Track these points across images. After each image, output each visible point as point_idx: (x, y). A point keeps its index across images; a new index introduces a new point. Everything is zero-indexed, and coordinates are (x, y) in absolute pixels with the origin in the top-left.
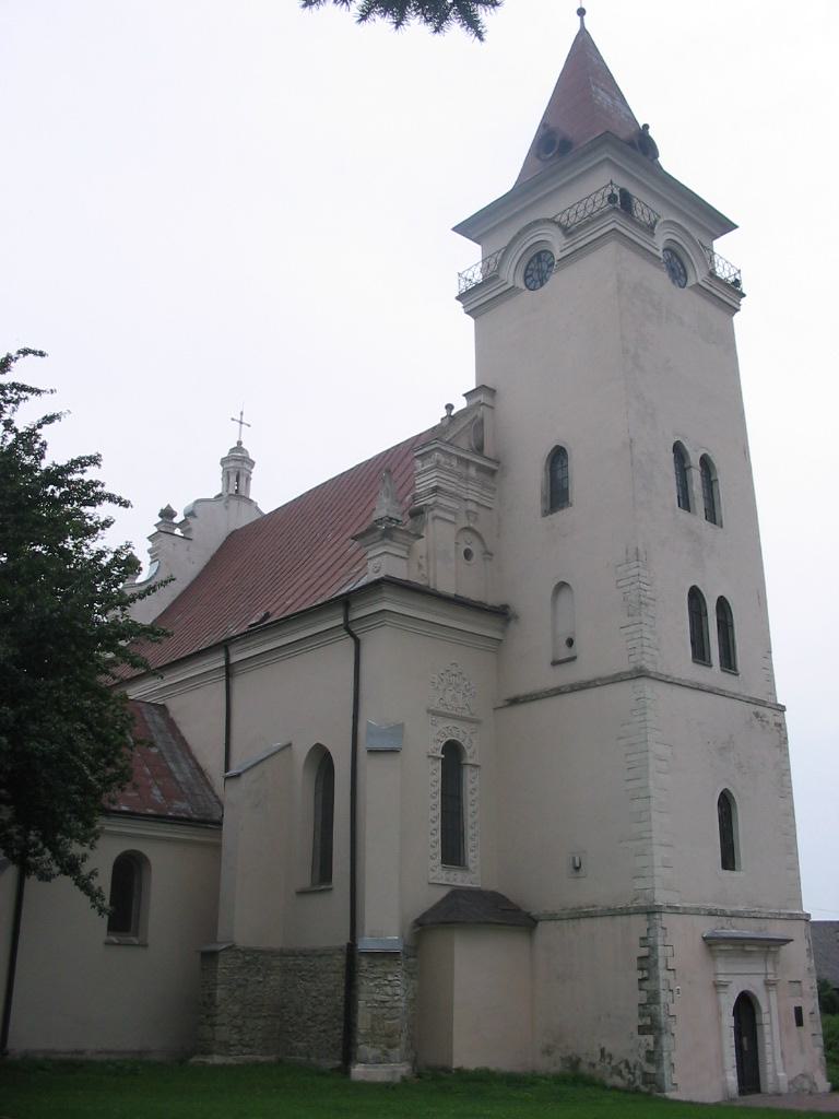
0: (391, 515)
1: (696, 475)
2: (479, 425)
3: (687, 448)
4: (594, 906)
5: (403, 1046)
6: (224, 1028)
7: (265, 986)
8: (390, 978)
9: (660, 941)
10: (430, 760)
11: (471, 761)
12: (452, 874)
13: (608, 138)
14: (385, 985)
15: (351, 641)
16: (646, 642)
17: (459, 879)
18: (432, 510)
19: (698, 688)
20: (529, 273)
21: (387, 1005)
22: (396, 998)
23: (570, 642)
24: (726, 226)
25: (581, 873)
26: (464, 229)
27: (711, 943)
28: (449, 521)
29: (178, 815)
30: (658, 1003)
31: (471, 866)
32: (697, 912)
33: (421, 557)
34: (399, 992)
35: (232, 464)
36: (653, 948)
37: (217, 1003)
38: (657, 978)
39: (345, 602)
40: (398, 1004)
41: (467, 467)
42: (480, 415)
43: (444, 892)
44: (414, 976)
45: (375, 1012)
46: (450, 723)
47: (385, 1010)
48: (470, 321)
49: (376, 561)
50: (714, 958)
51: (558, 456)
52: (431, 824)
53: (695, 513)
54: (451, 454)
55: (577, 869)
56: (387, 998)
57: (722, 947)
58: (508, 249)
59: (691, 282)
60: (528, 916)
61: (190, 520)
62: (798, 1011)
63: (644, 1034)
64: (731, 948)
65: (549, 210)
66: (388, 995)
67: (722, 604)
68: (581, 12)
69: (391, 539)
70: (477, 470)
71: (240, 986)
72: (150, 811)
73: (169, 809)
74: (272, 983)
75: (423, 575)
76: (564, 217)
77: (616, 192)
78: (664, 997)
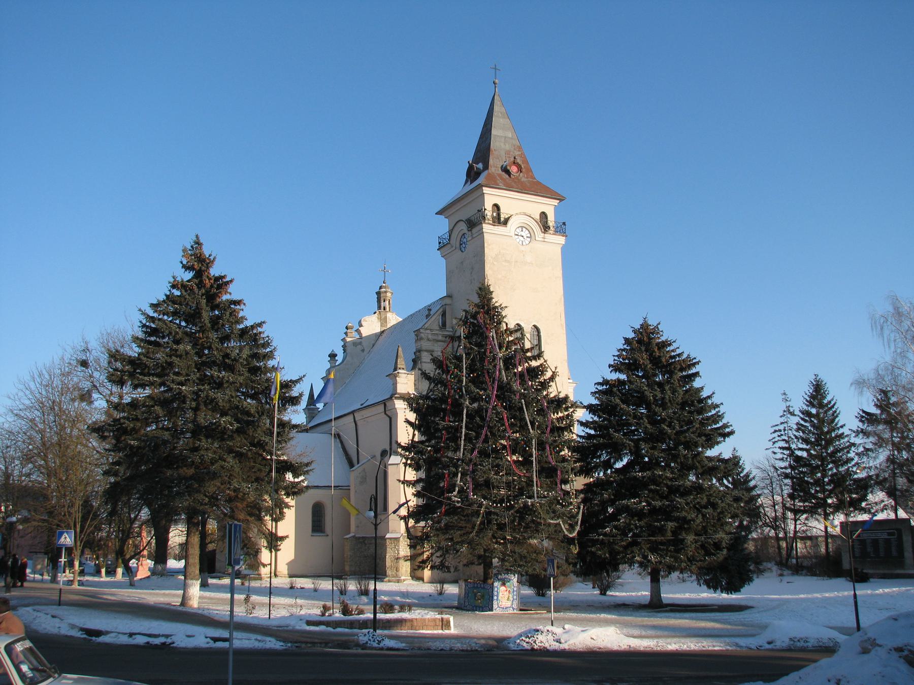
26: (439, 213)
48: (443, 261)
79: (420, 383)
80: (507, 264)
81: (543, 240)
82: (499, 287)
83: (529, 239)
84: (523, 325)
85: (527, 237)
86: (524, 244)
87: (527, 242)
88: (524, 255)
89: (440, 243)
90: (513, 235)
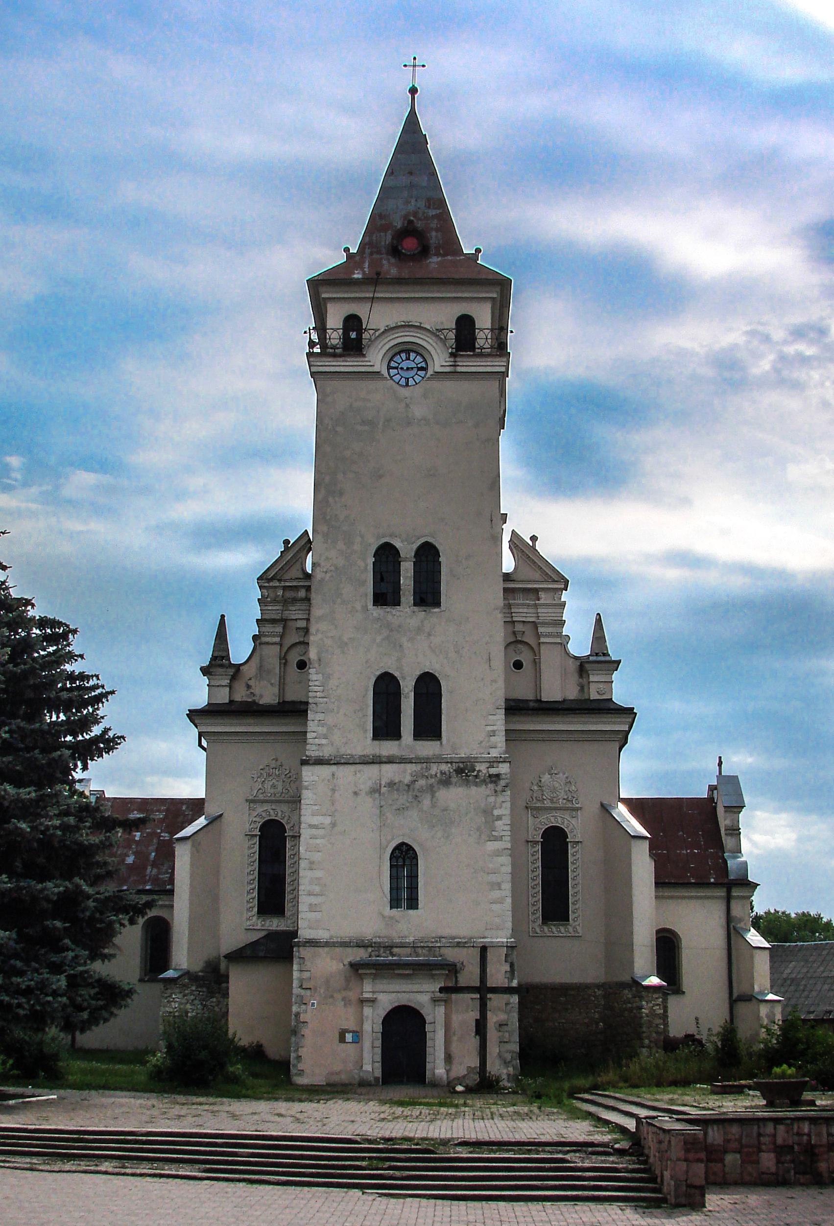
1: (407, 569)
8: (174, 996)
12: (268, 923)
32: (344, 944)
43: (263, 934)
46: (266, 807)
54: (276, 587)
59: (430, 372)
64: (374, 971)
75: (252, 693)
80: (366, 428)
81: (448, 369)
83: (422, 373)
84: (398, 544)
86: (411, 382)
88: (407, 406)
90: (385, 372)
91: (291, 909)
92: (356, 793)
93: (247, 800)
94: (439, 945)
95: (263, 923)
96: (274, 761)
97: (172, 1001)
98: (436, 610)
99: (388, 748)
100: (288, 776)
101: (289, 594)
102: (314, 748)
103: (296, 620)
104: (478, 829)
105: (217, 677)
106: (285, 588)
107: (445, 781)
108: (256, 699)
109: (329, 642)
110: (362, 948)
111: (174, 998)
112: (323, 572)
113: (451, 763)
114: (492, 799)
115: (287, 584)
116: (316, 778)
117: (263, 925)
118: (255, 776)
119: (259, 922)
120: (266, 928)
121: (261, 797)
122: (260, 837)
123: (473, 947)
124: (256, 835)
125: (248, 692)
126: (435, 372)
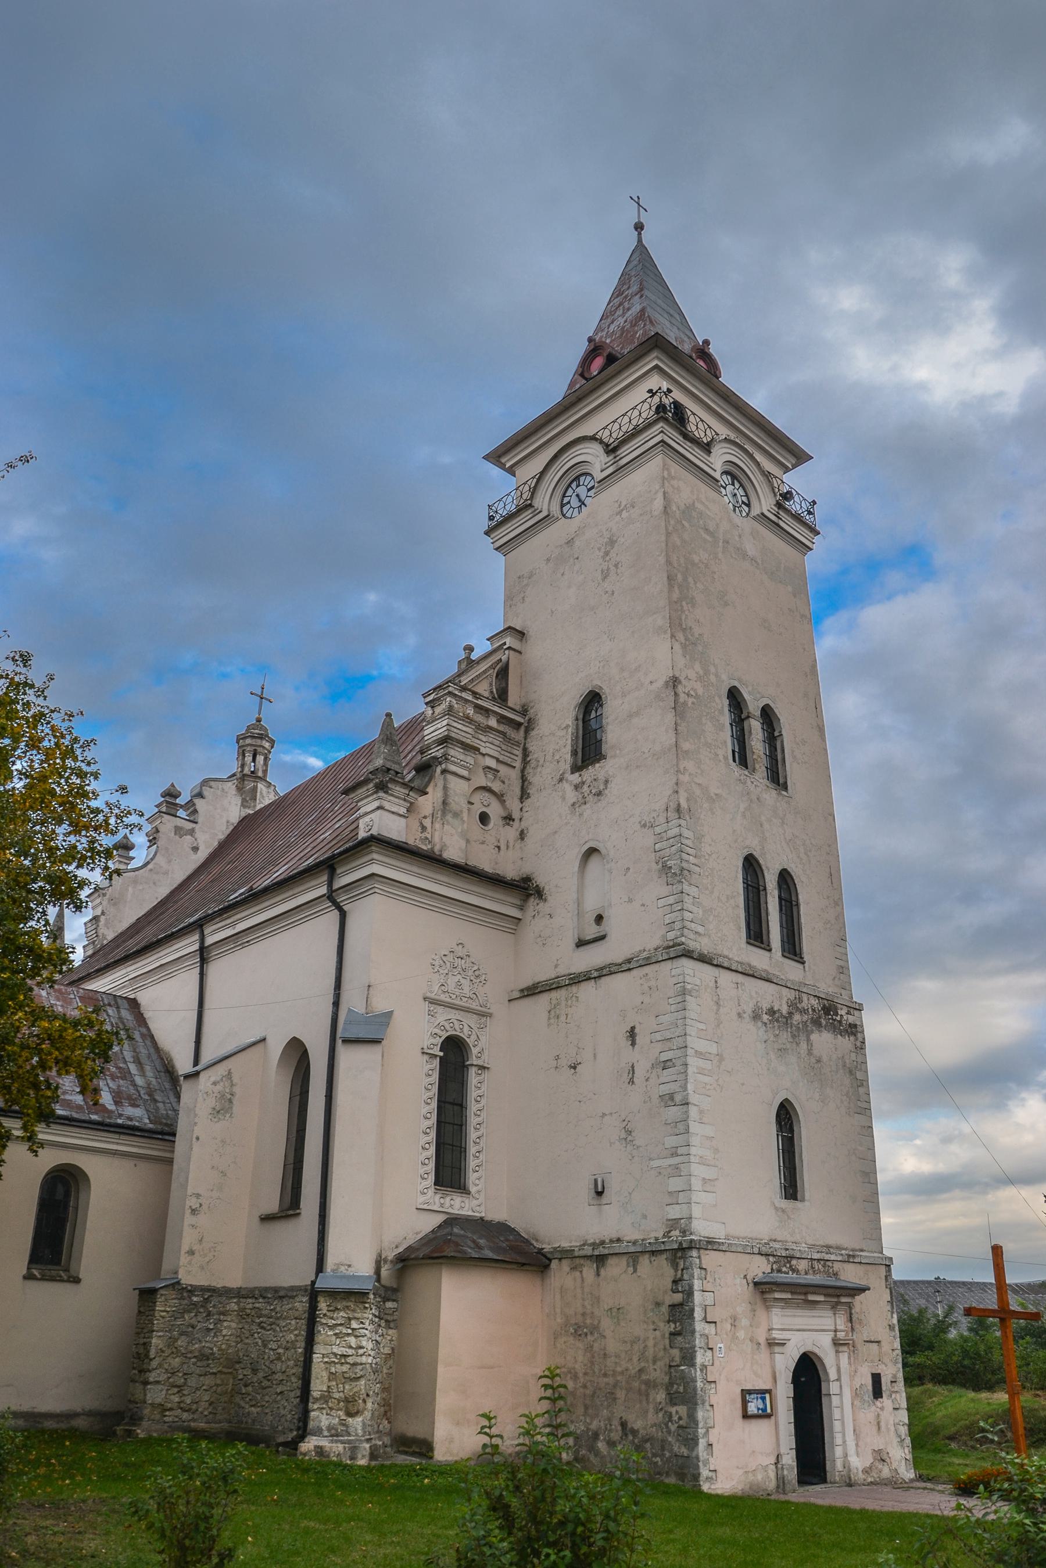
0: (389, 765)
1: (755, 728)
2: (503, 673)
3: (746, 696)
4: (619, 1240)
5: (368, 1414)
6: (160, 1387)
7: (215, 1335)
9: (697, 1284)
10: (426, 1057)
11: (480, 1062)
12: (448, 1199)
13: (657, 343)
14: (348, 1335)
15: (336, 913)
16: (687, 915)
17: (458, 1205)
18: (440, 763)
19: (750, 974)
20: (566, 500)
21: (350, 1360)
22: (361, 1351)
23: (599, 919)
24: (800, 457)
25: (605, 1199)
27: (763, 1288)
28: (463, 777)
29: (130, 1123)
30: (693, 1365)
31: (473, 1189)
33: (425, 817)
34: (364, 1343)
35: (248, 741)
36: (689, 1293)
37: (152, 1354)
38: (693, 1332)
39: (329, 866)
40: (364, 1359)
41: (488, 717)
42: (504, 658)
44: (392, 1325)
45: (333, 1370)
46: (453, 1015)
47: (345, 1368)
49: (367, 819)
50: (768, 1308)
51: (593, 700)
52: (422, 1135)
53: (754, 770)
54: (467, 701)
55: (599, 1194)
56: (350, 1352)
57: (777, 1295)
58: (543, 473)
59: (756, 511)
60: (540, 1251)
61: (197, 801)
62: (876, 1378)
63: (675, 1404)
64: (789, 1296)
65: (588, 429)
66: (351, 1347)
67: (785, 878)
68: (639, 227)
69: (386, 792)
70: (498, 721)
71: (183, 1333)
72: (94, 1117)
73: (120, 1115)
74: (224, 1332)
75: (427, 838)
76: (607, 433)
77: (666, 401)
78: (700, 1358)
79: (437, 826)
82: (695, 583)
85: (743, 502)
87: (744, 514)
89: (491, 518)
91: (477, 1182)
92: (739, 1015)
93: (425, 999)
94: (833, 1257)
95: (442, 1201)
96: (460, 946)
97: (348, 1335)
98: (784, 793)
99: (757, 958)
100: (477, 973)
101: (480, 718)
102: (692, 936)
103: (484, 755)
104: (847, 1094)
105: (392, 798)
106: (478, 708)
107: (817, 1023)
108: (437, 849)
109: (698, 792)
110: (763, 1258)
111: (353, 1329)
112: (684, 693)
113: (819, 997)
114: (853, 1055)
115: (479, 702)
116: (698, 982)
117: (442, 1205)
118: (437, 963)
119: (438, 1196)
120: (446, 1210)
121: (443, 997)
122: (441, 1058)
123: (861, 1263)
124: (436, 1056)
125: (423, 835)
126: (763, 514)
